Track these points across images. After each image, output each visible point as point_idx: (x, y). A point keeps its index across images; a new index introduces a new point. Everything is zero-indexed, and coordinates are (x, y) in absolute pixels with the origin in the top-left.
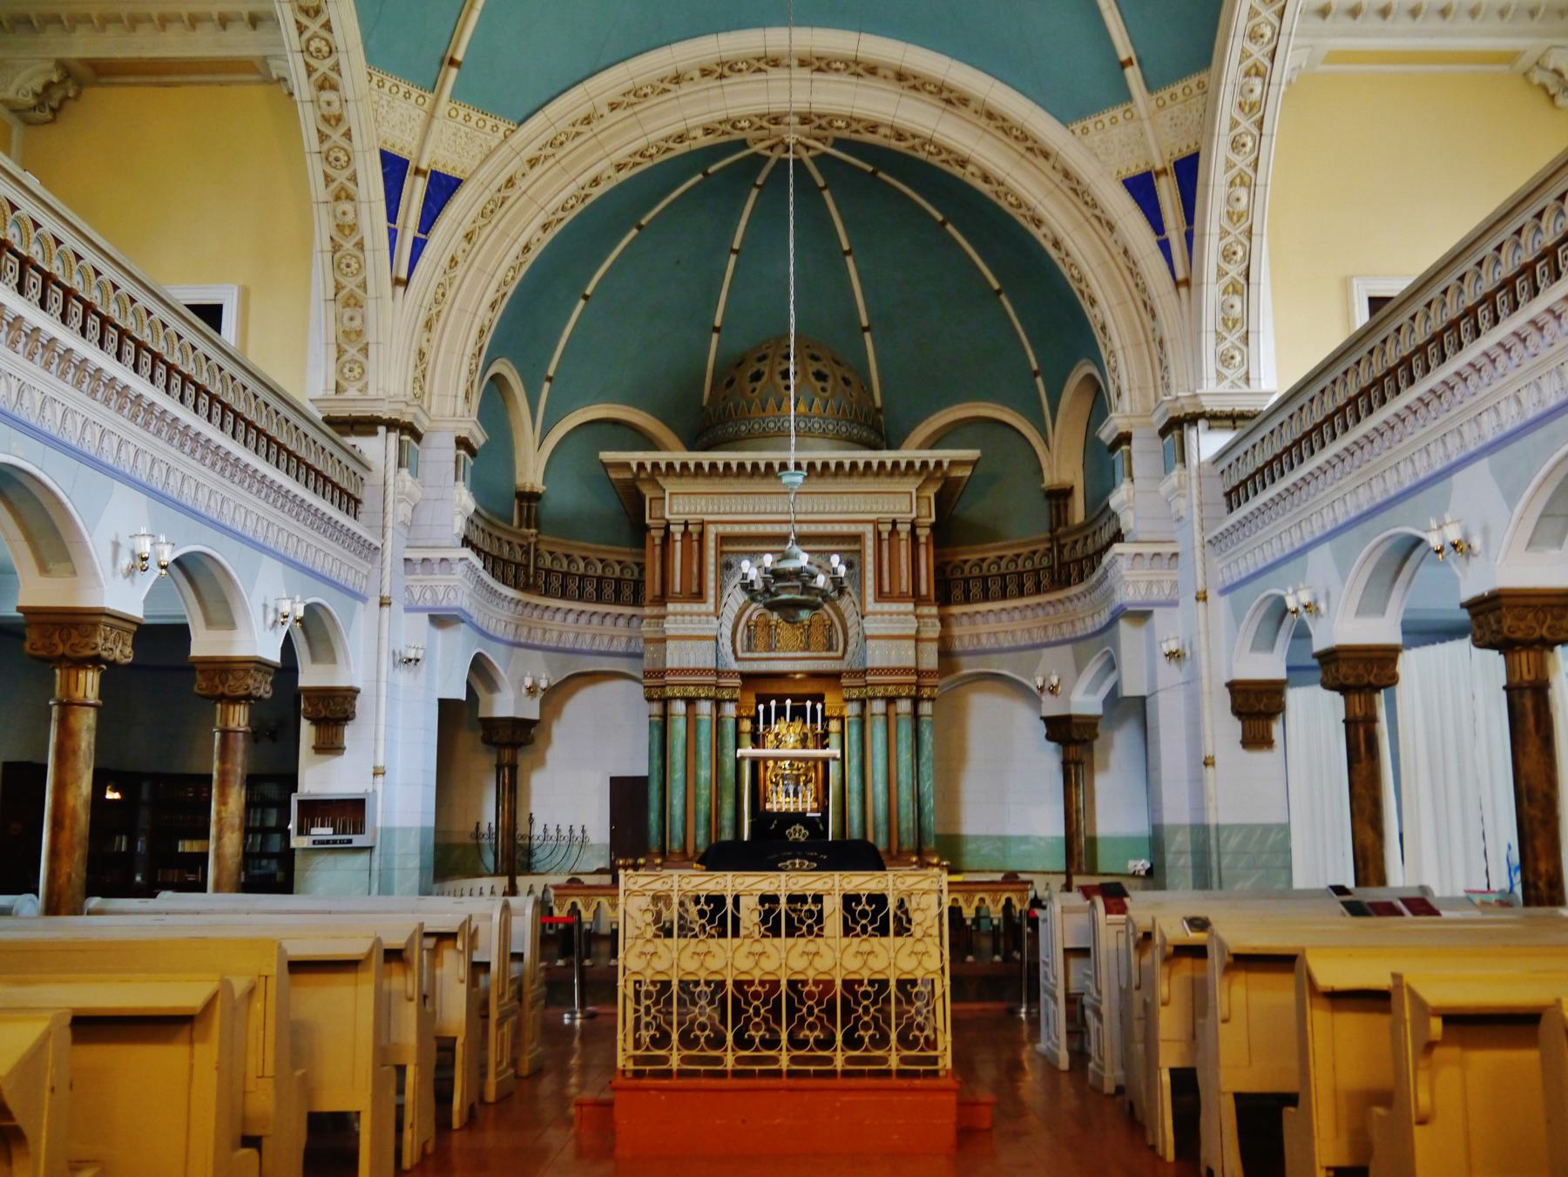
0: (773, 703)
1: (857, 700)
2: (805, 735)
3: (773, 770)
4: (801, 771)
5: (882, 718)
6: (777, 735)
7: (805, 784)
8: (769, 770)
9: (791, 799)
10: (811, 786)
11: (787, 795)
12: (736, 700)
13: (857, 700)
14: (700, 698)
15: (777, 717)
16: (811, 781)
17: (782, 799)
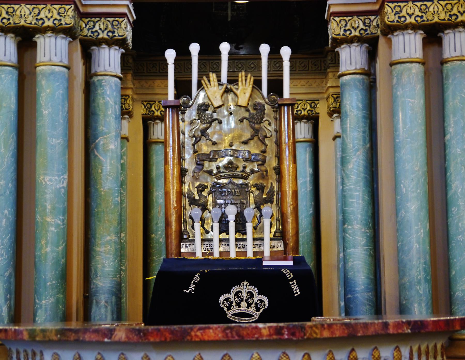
0: (195, 48)
1: (360, 40)
2: (259, 108)
3: (195, 178)
4: (252, 180)
5: (417, 69)
6: (203, 108)
7: (258, 208)
8: (188, 179)
9: (232, 235)
10: (267, 209)
11: (224, 228)
12: (121, 43)
13: (360, 40)
14: (43, 30)
15: (202, 72)
16: (269, 200)
17: (215, 235)
